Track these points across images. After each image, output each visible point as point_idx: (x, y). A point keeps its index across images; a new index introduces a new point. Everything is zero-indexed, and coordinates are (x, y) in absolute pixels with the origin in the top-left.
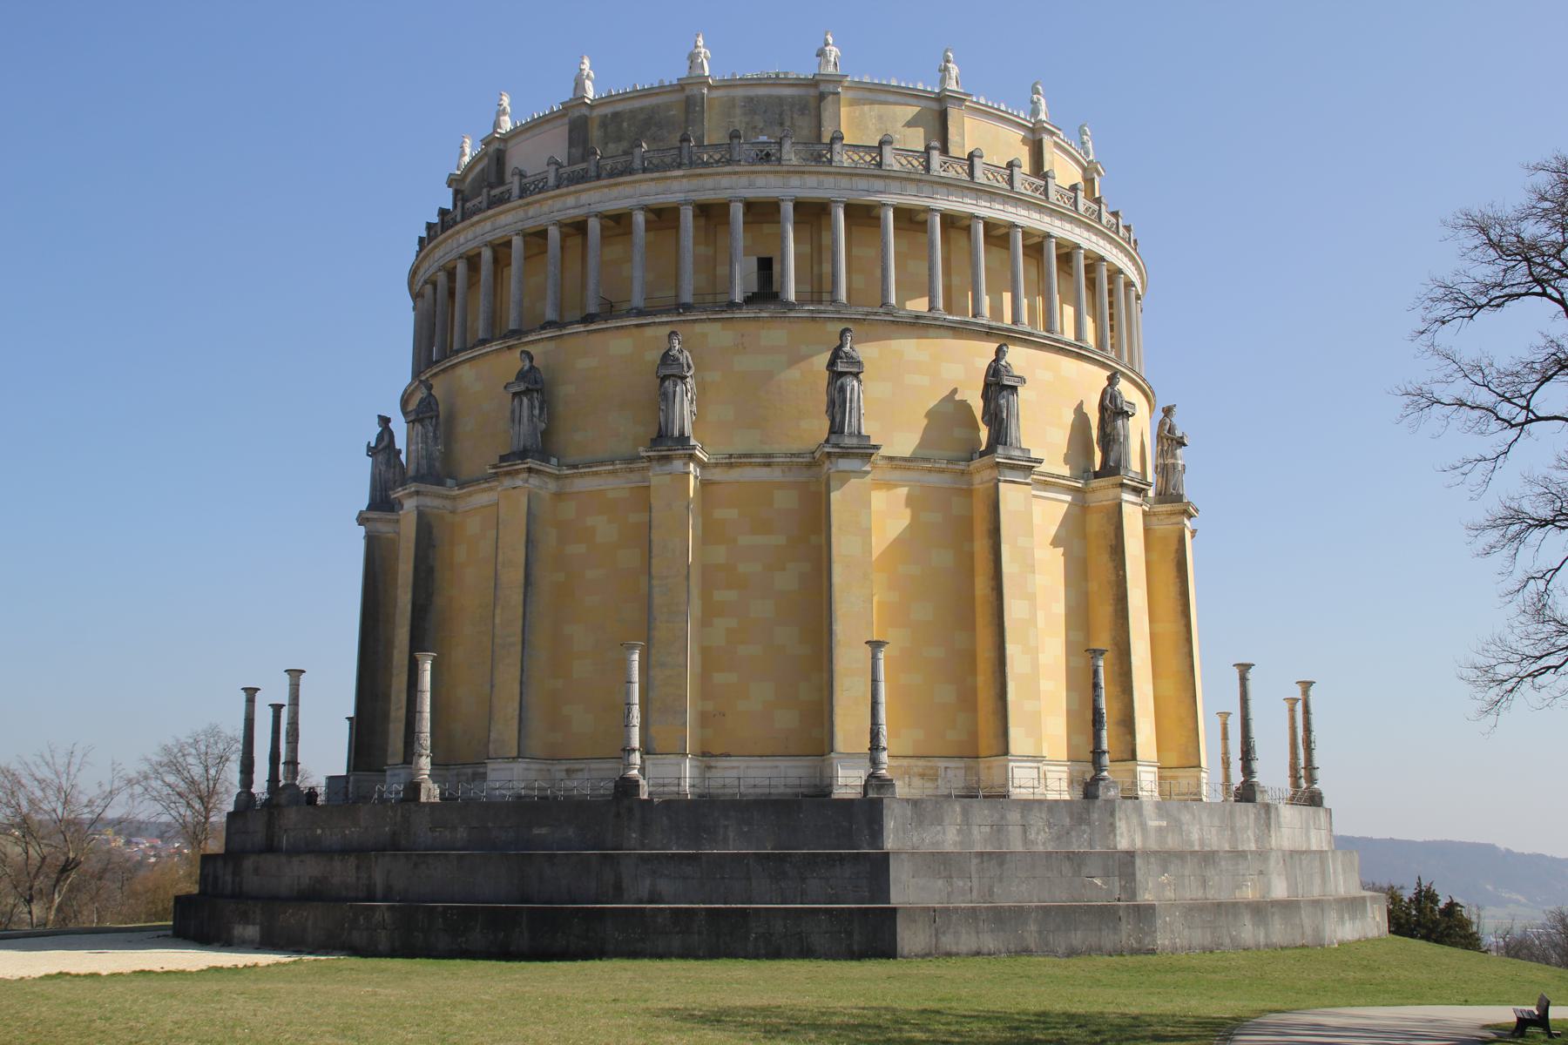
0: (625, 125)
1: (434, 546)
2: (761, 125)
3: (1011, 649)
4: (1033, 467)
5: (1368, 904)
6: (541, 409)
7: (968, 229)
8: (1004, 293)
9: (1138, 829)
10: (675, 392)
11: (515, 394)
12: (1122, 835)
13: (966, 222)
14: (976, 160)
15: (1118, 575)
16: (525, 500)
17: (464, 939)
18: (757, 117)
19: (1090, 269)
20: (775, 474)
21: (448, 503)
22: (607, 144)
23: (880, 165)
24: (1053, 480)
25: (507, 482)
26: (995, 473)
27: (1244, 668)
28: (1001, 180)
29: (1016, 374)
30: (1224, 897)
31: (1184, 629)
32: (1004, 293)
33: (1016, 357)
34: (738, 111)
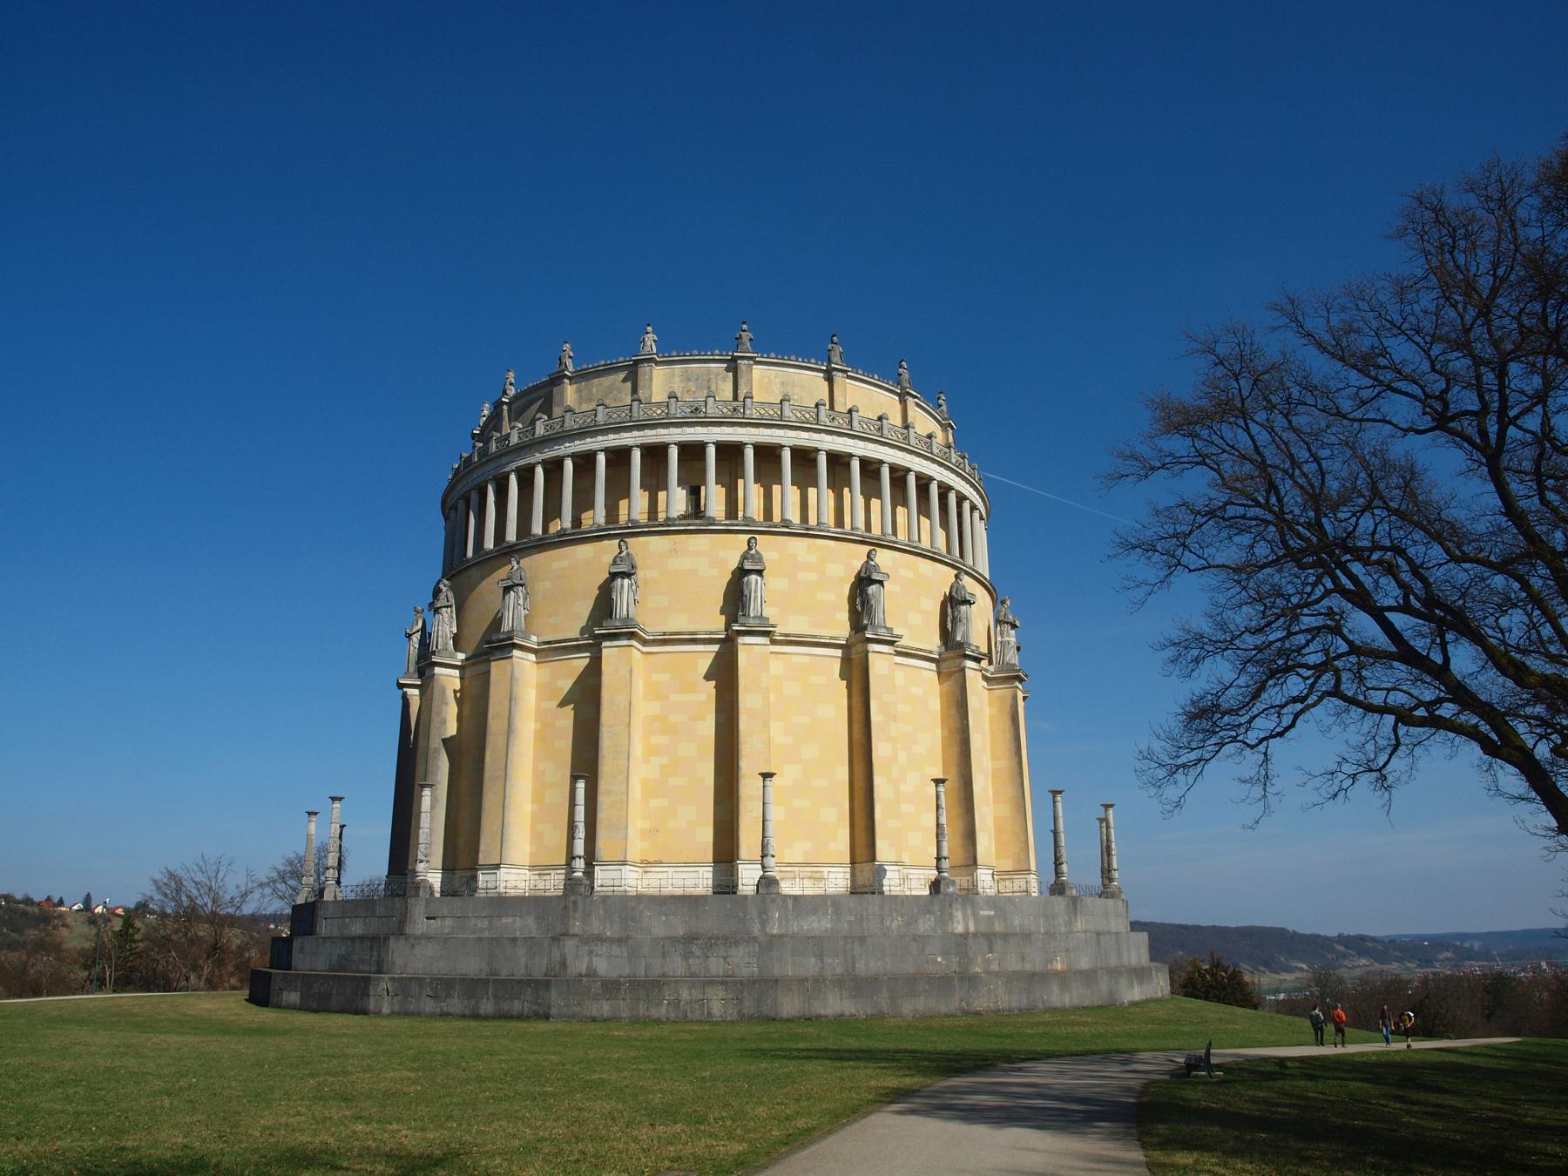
0: (594, 390)
1: (447, 704)
2: (693, 389)
3: (878, 780)
4: (896, 641)
5: (1154, 973)
6: (525, 599)
7: (848, 466)
8: (774, 486)
9: (971, 917)
10: (622, 585)
12: (958, 922)
13: (874, 466)
15: (963, 724)
17: (445, 1004)
18: (690, 383)
19: (943, 497)
22: (581, 404)
24: (913, 652)
28: (872, 428)
29: (882, 571)
30: (1039, 968)
31: (1016, 766)
32: (774, 486)
33: (884, 558)
34: (677, 379)
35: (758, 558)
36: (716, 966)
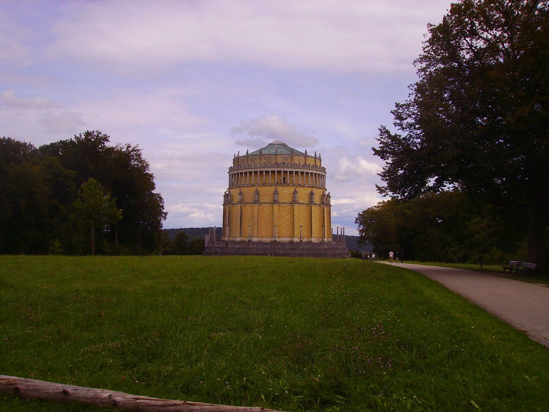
11: (255, 194)
14: (310, 166)
16: (257, 207)
20: (287, 205)
21: (243, 205)
23: (299, 167)
25: (255, 204)
26: (311, 205)
27: (338, 227)
35: (296, 191)
36: (295, 252)
